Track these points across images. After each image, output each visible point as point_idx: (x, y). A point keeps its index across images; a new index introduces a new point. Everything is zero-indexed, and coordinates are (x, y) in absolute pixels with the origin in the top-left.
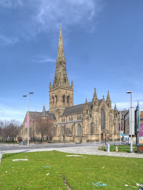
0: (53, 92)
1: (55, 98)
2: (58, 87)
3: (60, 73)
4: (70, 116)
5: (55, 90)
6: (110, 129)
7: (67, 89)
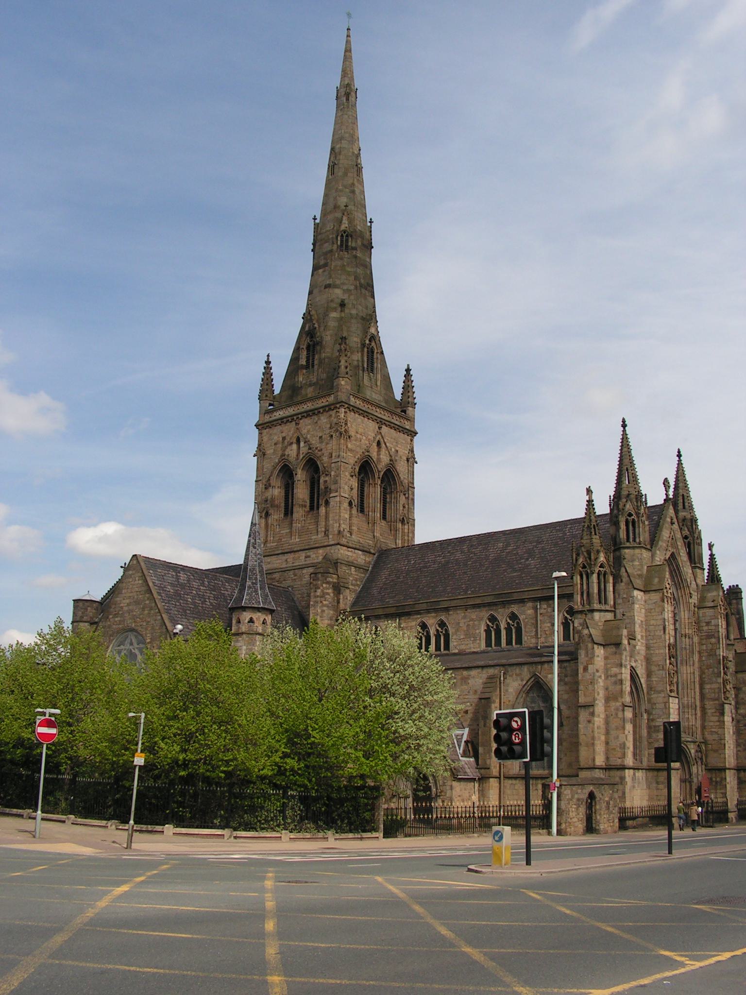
0: (289, 430)
1: (300, 475)
2: (331, 399)
3: (342, 305)
4: (432, 622)
5: (308, 414)
6: (703, 727)
7: (386, 416)
